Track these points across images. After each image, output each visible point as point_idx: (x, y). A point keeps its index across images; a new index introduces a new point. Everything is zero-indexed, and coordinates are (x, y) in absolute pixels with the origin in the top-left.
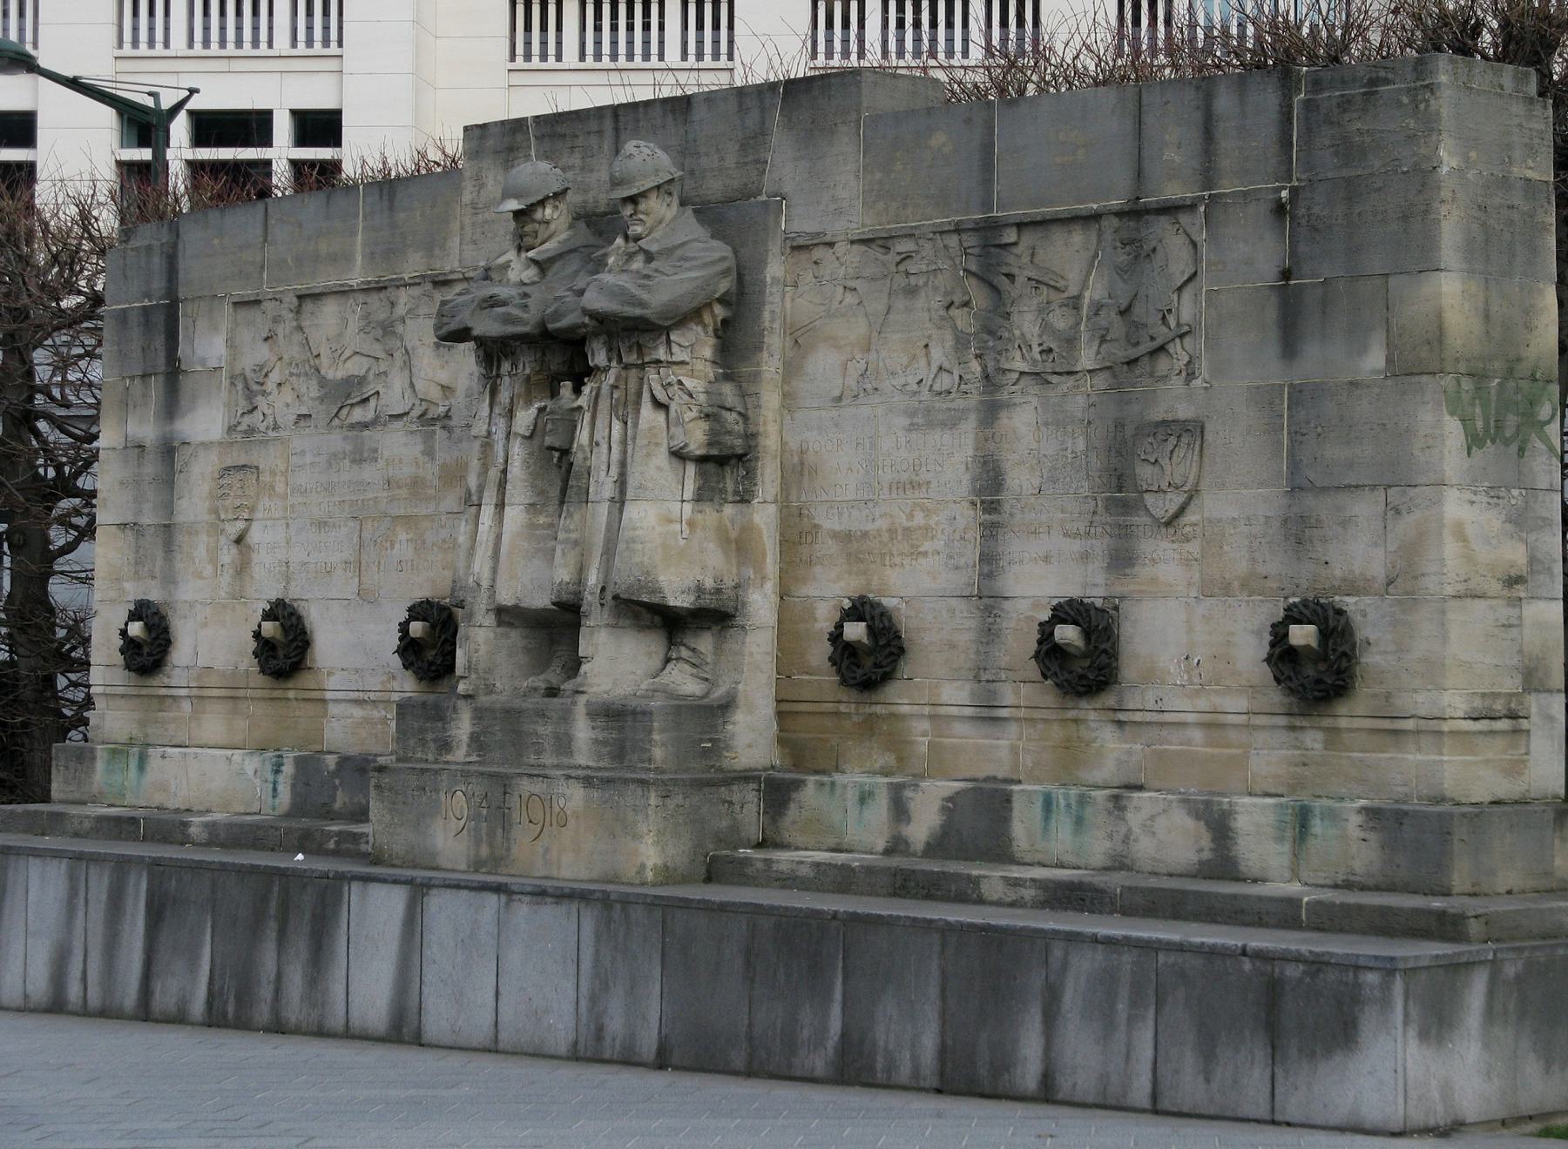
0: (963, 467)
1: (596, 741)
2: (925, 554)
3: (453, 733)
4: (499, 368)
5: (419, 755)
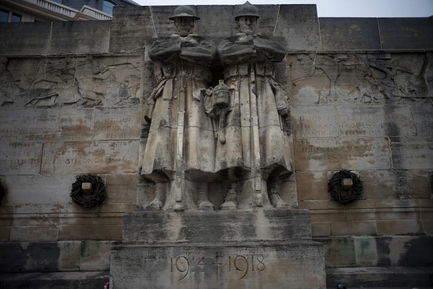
0: (380, 127)
1: (273, 228)
2: (367, 155)
5: (141, 240)
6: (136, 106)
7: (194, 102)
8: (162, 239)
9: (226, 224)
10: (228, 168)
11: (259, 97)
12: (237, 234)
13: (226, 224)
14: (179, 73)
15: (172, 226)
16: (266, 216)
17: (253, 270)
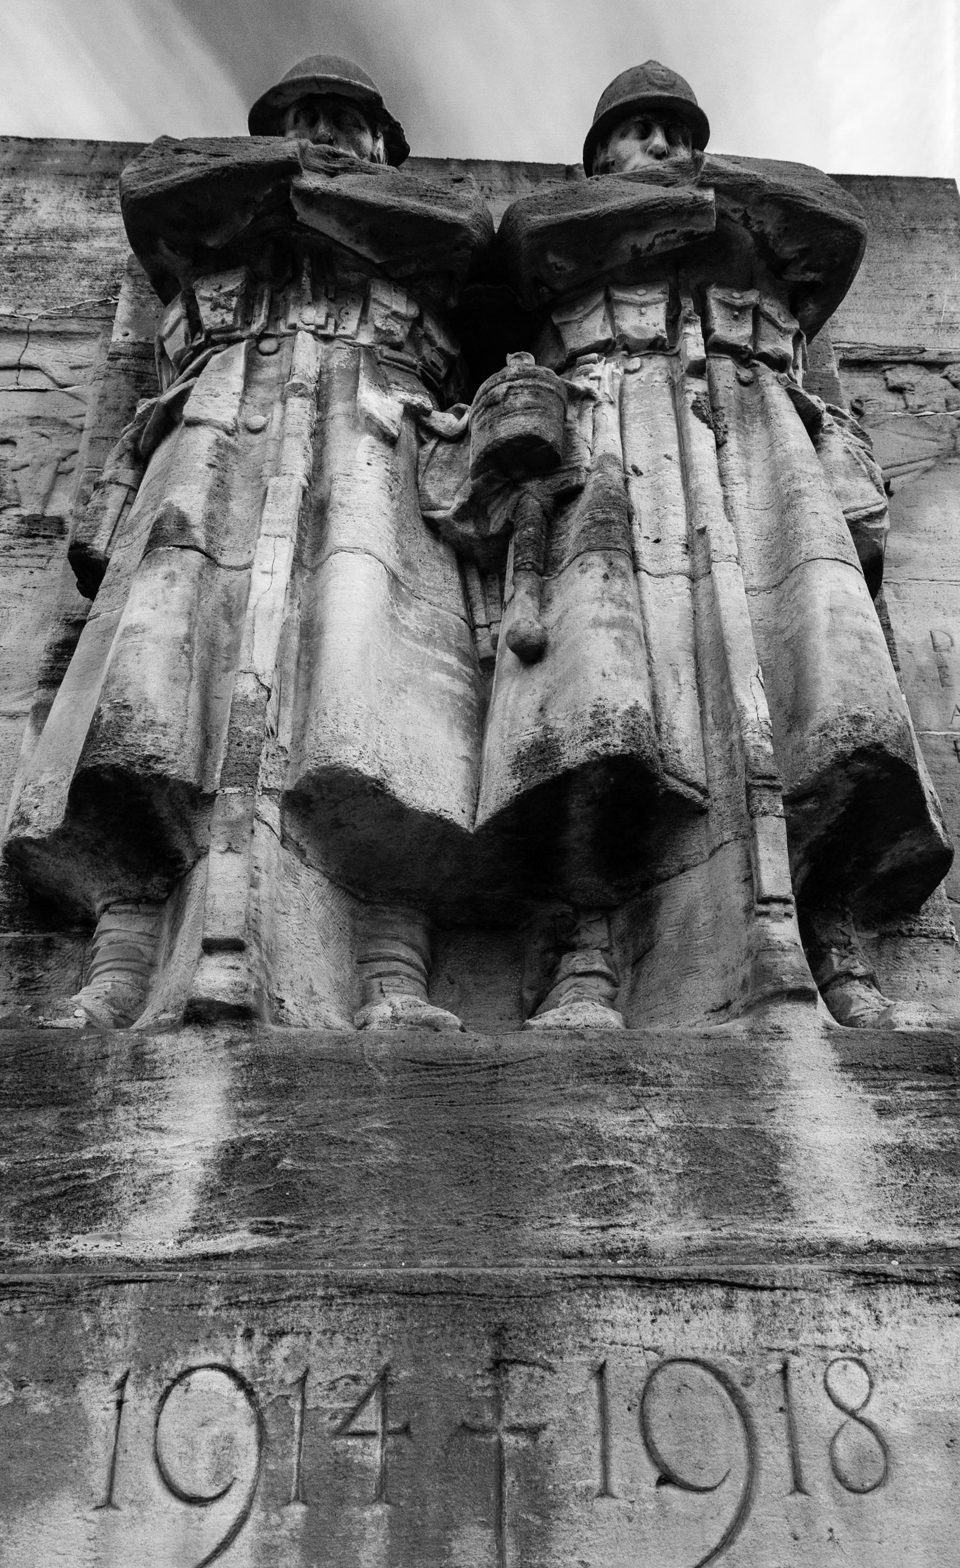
3: (122, 1149)
4: (275, 316)
6: (40, 550)
7: (368, 440)
8: (67, 1230)
9: (563, 1117)
10: (568, 773)
11: (732, 444)
12: (644, 1196)
13: (563, 1117)
14: (285, 315)
15: (160, 1130)
16: (845, 1066)
17: (798, 1486)
